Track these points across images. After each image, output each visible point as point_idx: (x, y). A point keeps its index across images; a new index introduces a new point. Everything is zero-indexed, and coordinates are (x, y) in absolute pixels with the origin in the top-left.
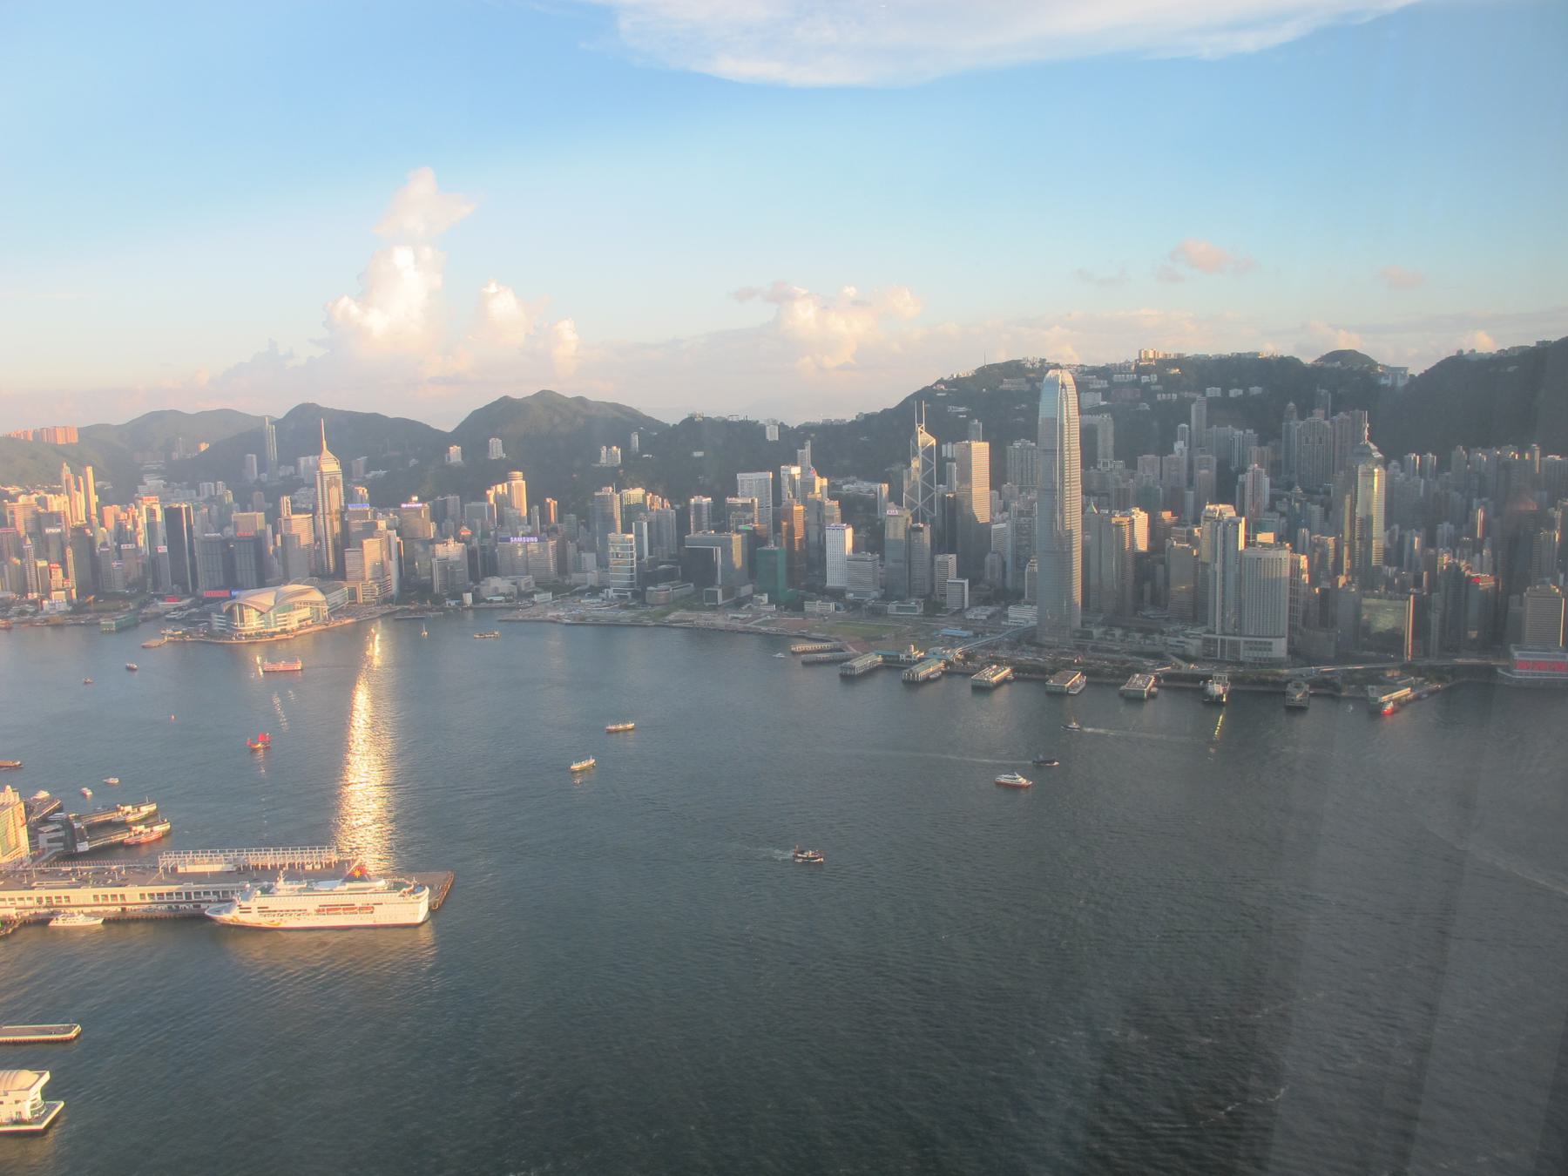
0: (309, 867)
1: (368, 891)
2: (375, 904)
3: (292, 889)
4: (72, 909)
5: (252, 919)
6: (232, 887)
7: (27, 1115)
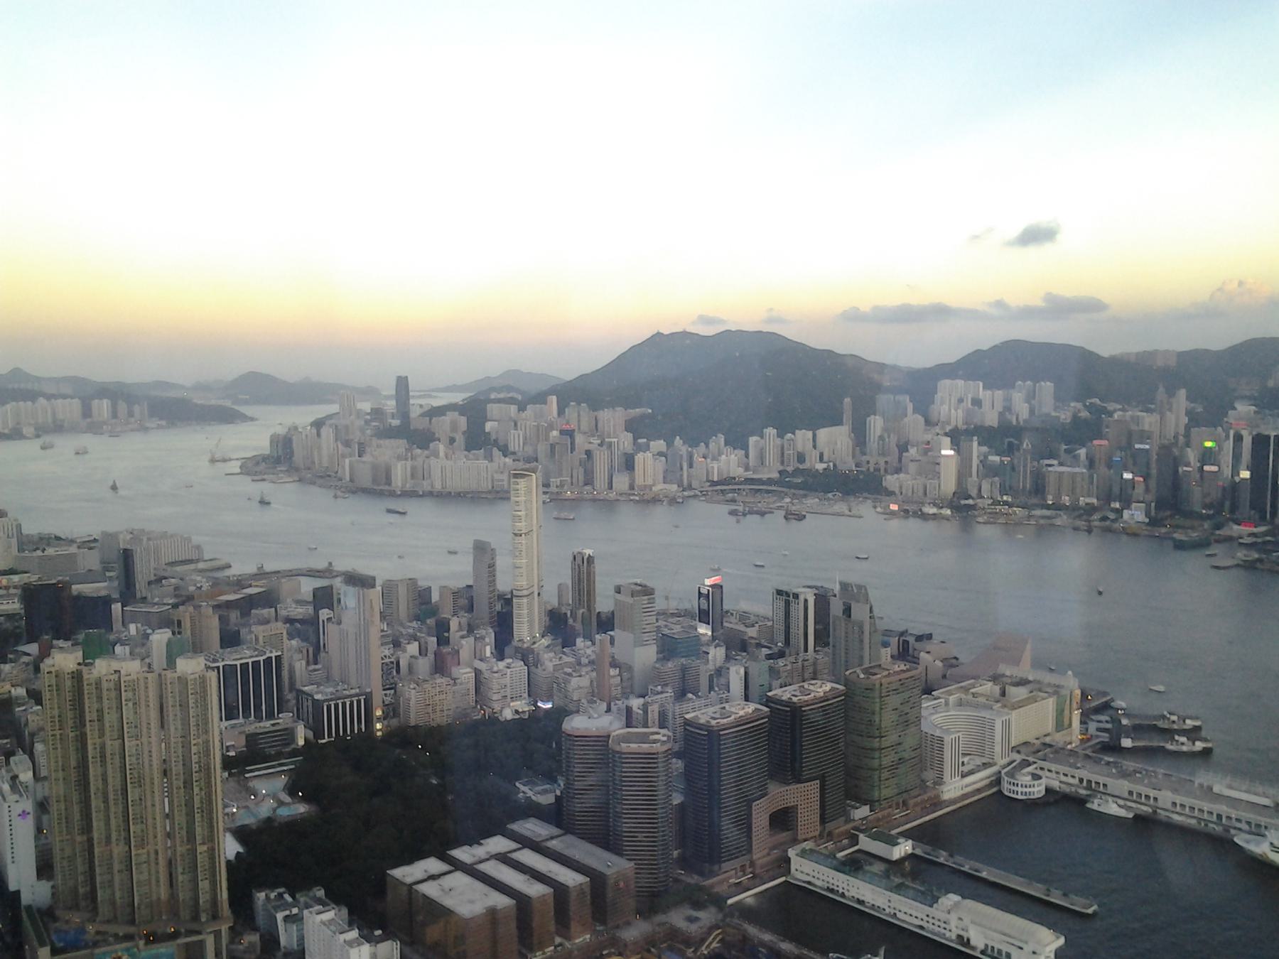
4: (1107, 797)
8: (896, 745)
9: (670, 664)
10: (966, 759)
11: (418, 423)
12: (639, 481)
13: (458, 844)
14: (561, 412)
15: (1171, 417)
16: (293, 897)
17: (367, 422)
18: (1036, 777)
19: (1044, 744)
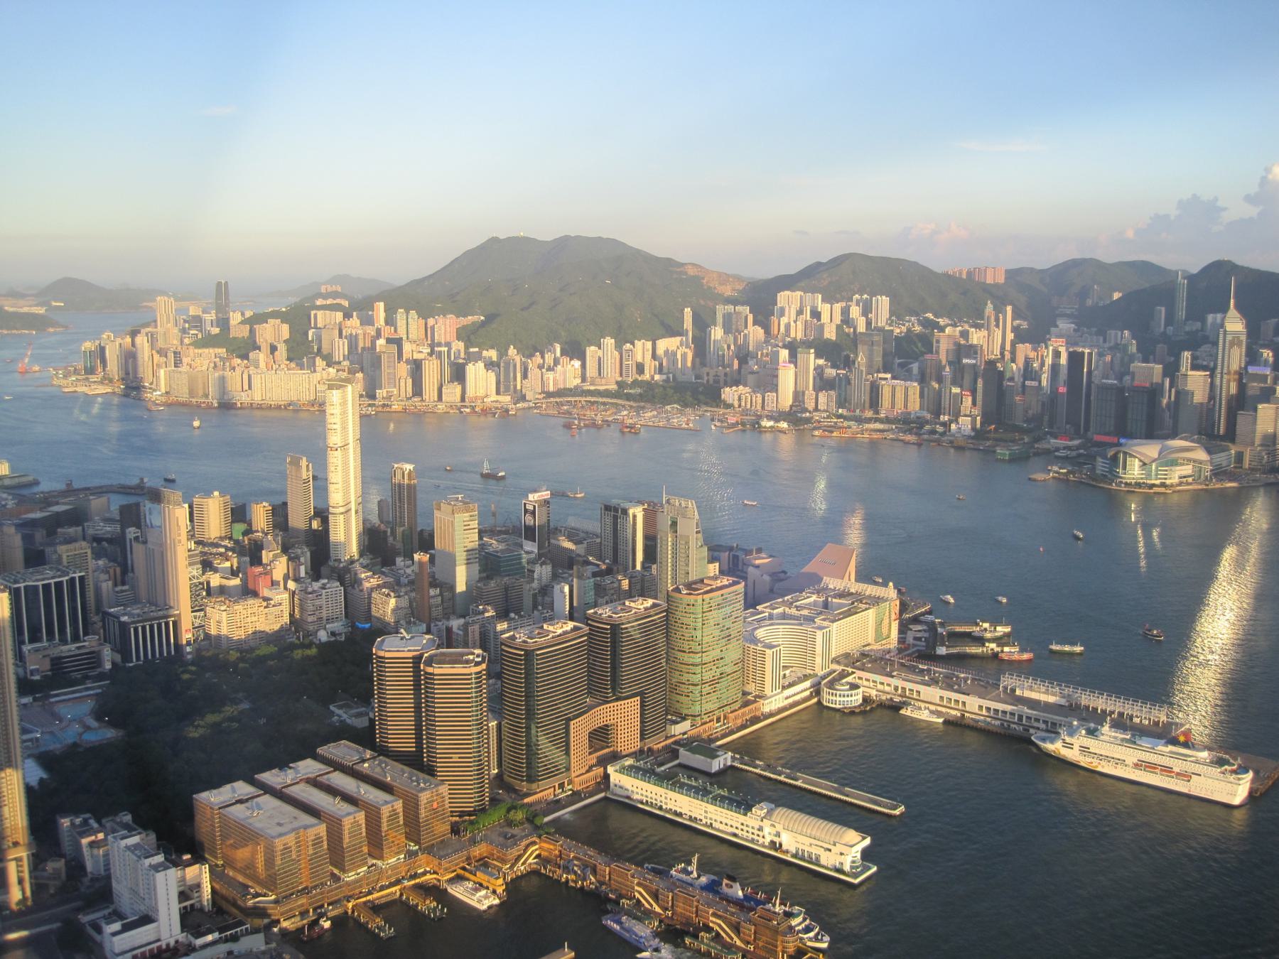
0: (1137, 720)
1: (1189, 759)
2: (1193, 773)
3: (1115, 738)
5: (1072, 755)
6: (1061, 721)
7: (847, 868)
8: (718, 660)
9: (492, 584)
10: (787, 672)
11: (238, 330)
12: (470, 392)
13: (269, 767)
14: (390, 321)
15: (998, 334)
16: (99, 822)
17: (184, 331)
18: (854, 687)
19: (864, 655)
